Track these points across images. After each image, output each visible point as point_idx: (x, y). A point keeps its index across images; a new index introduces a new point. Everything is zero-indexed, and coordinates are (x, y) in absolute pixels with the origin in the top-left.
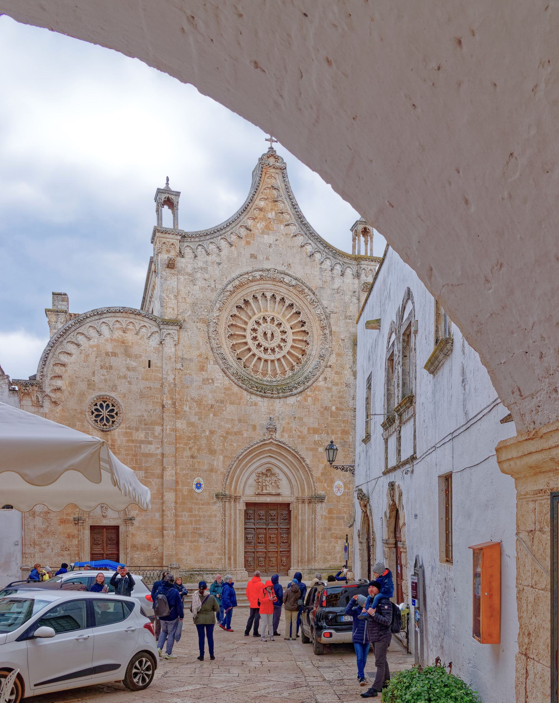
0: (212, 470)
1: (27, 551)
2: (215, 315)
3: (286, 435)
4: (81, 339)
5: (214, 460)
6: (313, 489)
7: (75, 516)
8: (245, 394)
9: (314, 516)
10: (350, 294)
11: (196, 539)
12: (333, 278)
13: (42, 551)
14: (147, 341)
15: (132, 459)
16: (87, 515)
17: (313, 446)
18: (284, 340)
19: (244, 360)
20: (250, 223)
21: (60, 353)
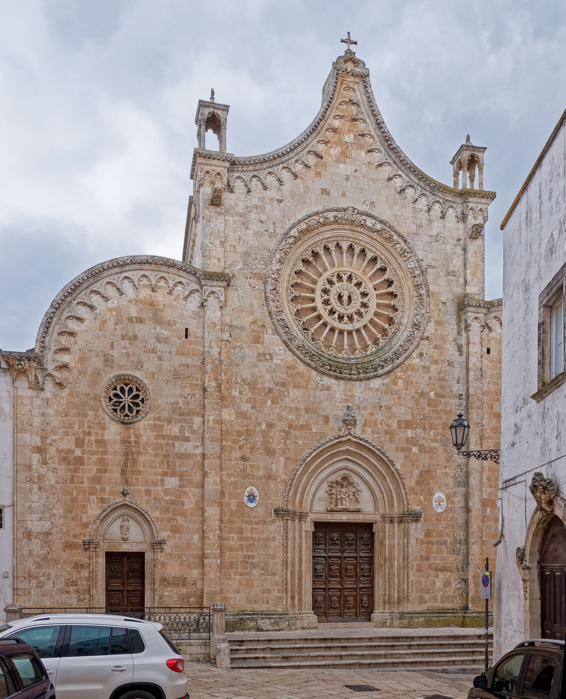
0: (269, 477)
1: (20, 586)
2: (274, 268)
3: (369, 430)
4: (95, 300)
5: (272, 463)
6: (405, 503)
7: (85, 539)
8: (315, 375)
9: (406, 540)
10: (453, 242)
11: (248, 570)
13: (40, 586)
14: (184, 303)
15: (162, 462)
16: (102, 538)
17: (405, 445)
18: (364, 305)
19: (312, 330)
20: (321, 148)
21: (68, 318)
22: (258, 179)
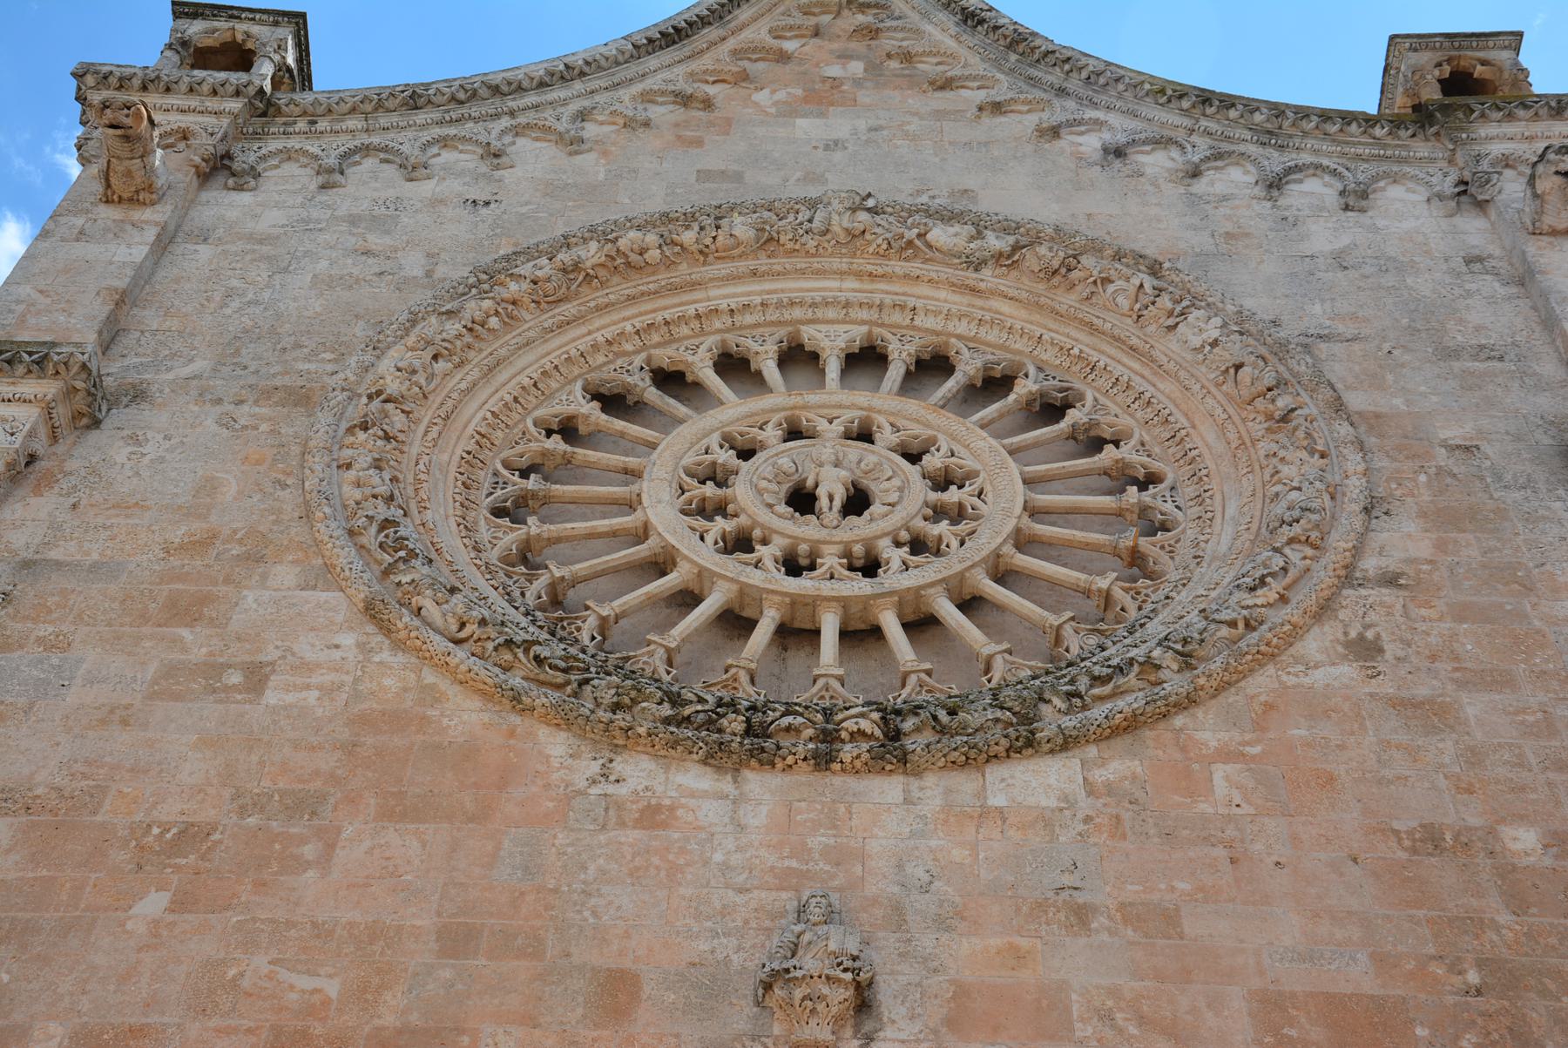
12: (1287, 222)
22: (382, 155)
